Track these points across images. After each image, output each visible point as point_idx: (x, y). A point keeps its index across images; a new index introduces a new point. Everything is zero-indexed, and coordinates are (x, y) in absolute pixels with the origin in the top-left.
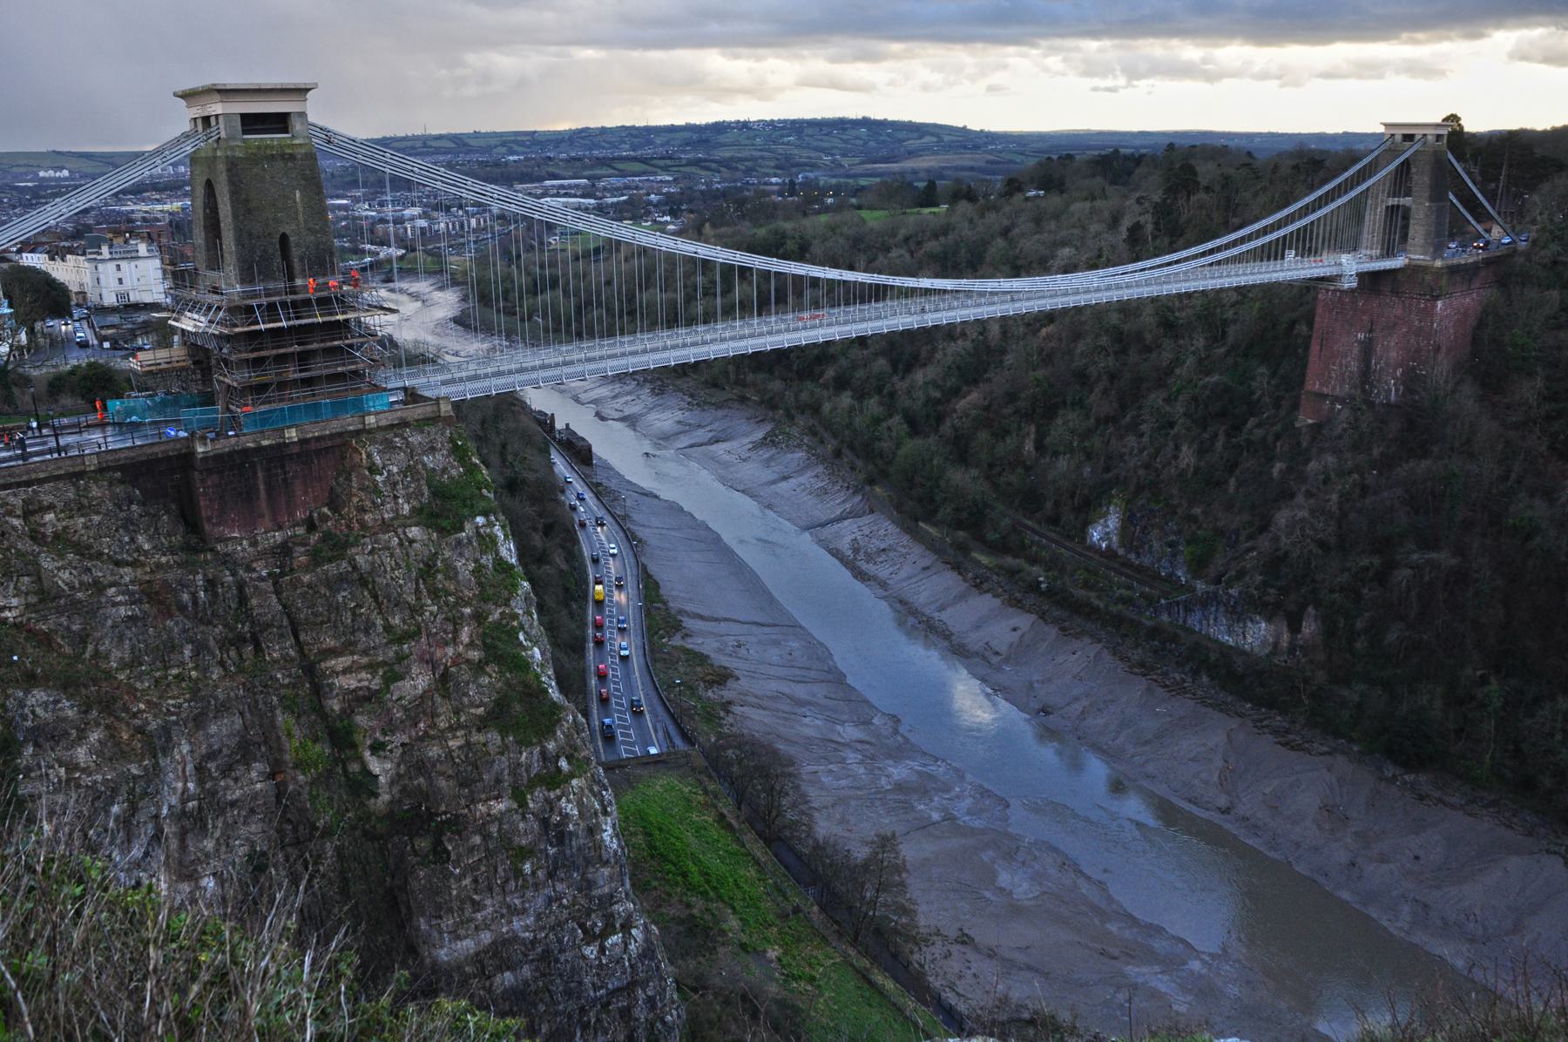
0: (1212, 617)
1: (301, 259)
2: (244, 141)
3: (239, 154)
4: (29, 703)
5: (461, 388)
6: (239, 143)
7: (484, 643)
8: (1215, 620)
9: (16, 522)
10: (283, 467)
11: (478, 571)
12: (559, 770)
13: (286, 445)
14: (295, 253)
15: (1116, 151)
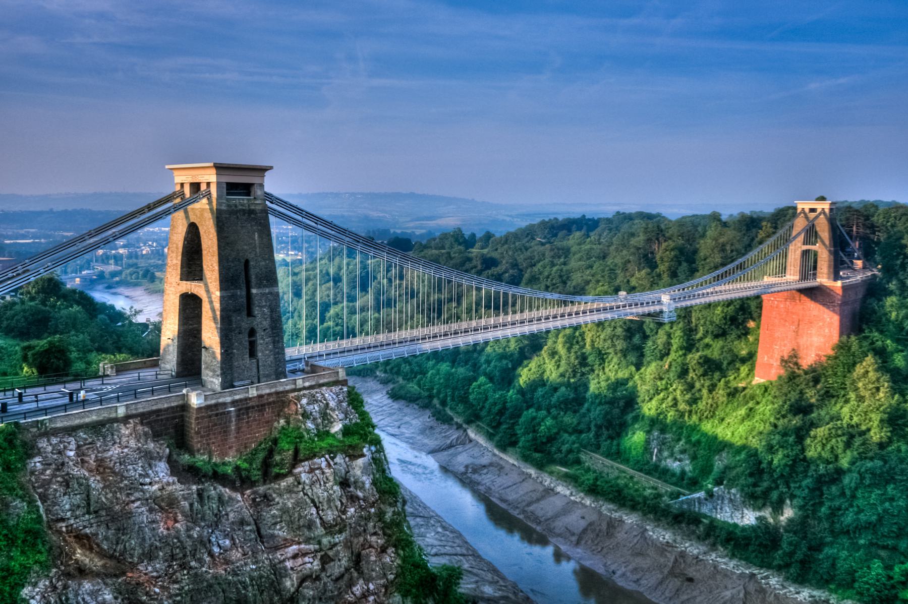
0: (719, 507)
1: (257, 277)
2: (227, 200)
4: (80, 592)
5: (338, 361)
6: (224, 201)
7: (385, 534)
8: (721, 509)
9: (72, 454)
10: (248, 414)
11: (374, 483)
13: (250, 399)
14: (253, 273)
15: (584, 216)
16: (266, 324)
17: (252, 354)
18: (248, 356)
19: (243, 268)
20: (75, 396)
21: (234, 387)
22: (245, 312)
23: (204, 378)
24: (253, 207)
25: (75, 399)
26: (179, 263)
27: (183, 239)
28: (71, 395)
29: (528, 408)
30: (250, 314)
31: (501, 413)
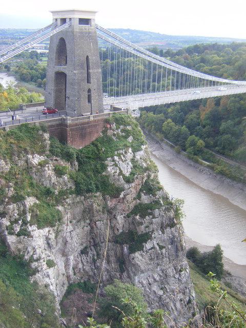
12: (174, 222)
14: (90, 61)
16: (95, 87)
17: (89, 101)
20: (14, 117)
21: (83, 116)
24: (90, 30)
25: (15, 119)
26: (54, 57)
28: (13, 117)
29: (191, 134)
30: (88, 82)
31: (178, 136)
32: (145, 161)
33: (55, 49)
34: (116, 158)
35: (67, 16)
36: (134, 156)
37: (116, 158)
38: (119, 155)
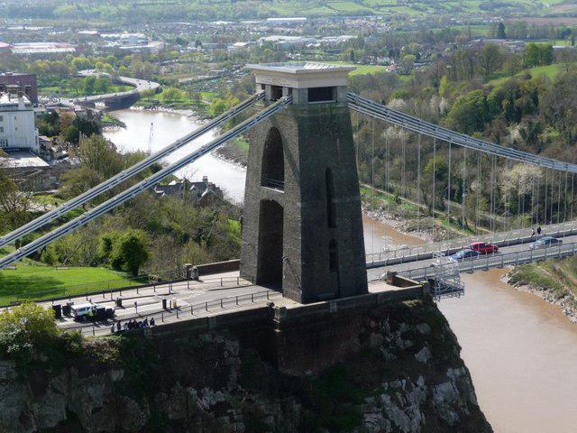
3: (305, 115)
6: (306, 108)
17: (333, 266)
18: (328, 268)
19: (324, 178)
22: (326, 223)
23: (284, 288)
24: (334, 112)
27: (263, 143)
30: (331, 224)
32: (454, 407)
33: (262, 150)
34: (385, 398)
35: (286, 83)
36: (430, 397)
37: (385, 398)
38: (391, 392)
